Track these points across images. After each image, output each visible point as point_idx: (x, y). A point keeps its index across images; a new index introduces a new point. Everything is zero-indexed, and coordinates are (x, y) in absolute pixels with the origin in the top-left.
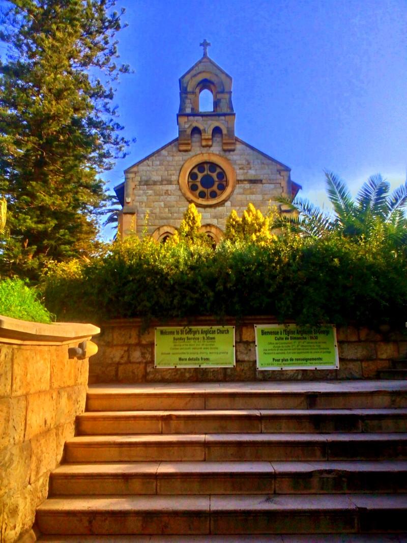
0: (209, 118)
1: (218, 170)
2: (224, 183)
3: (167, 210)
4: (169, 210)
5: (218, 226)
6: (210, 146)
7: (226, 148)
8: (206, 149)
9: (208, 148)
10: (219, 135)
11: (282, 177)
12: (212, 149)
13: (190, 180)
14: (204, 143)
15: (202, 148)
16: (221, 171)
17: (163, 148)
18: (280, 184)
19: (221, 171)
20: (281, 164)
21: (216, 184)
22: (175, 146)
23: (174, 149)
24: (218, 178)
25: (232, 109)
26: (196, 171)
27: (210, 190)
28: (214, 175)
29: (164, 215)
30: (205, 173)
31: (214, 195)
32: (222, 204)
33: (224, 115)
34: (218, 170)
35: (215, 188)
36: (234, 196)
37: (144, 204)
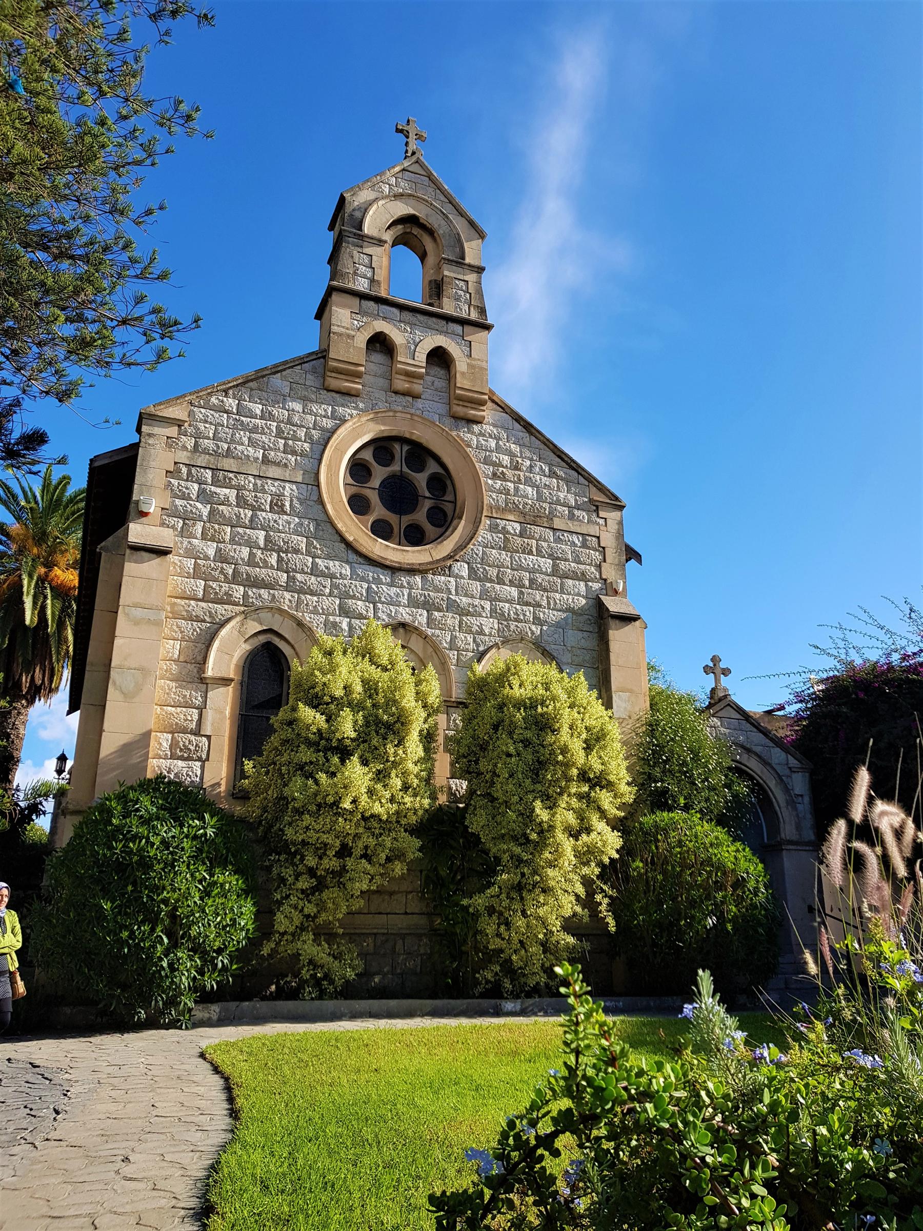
0: (421, 317)
1: (432, 467)
2: (448, 508)
3: (273, 560)
4: (280, 560)
5: (430, 632)
6: (416, 397)
7: (460, 410)
8: (400, 399)
9: (410, 399)
10: (442, 372)
11: (602, 522)
12: (419, 403)
13: (350, 481)
14: (401, 384)
15: (394, 397)
16: (440, 470)
17: (277, 369)
18: (598, 538)
19: (440, 470)
20: (601, 488)
21: (428, 504)
22: (314, 371)
23: (311, 380)
24: (429, 487)
25: (482, 311)
26: (368, 455)
27: (406, 520)
28: (421, 479)
29: (261, 573)
30: (395, 467)
31: (415, 537)
32: (442, 567)
33: (463, 322)
34: (432, 467)
35: (420, 516)
36: (477, 550)
37: (199, 527)
